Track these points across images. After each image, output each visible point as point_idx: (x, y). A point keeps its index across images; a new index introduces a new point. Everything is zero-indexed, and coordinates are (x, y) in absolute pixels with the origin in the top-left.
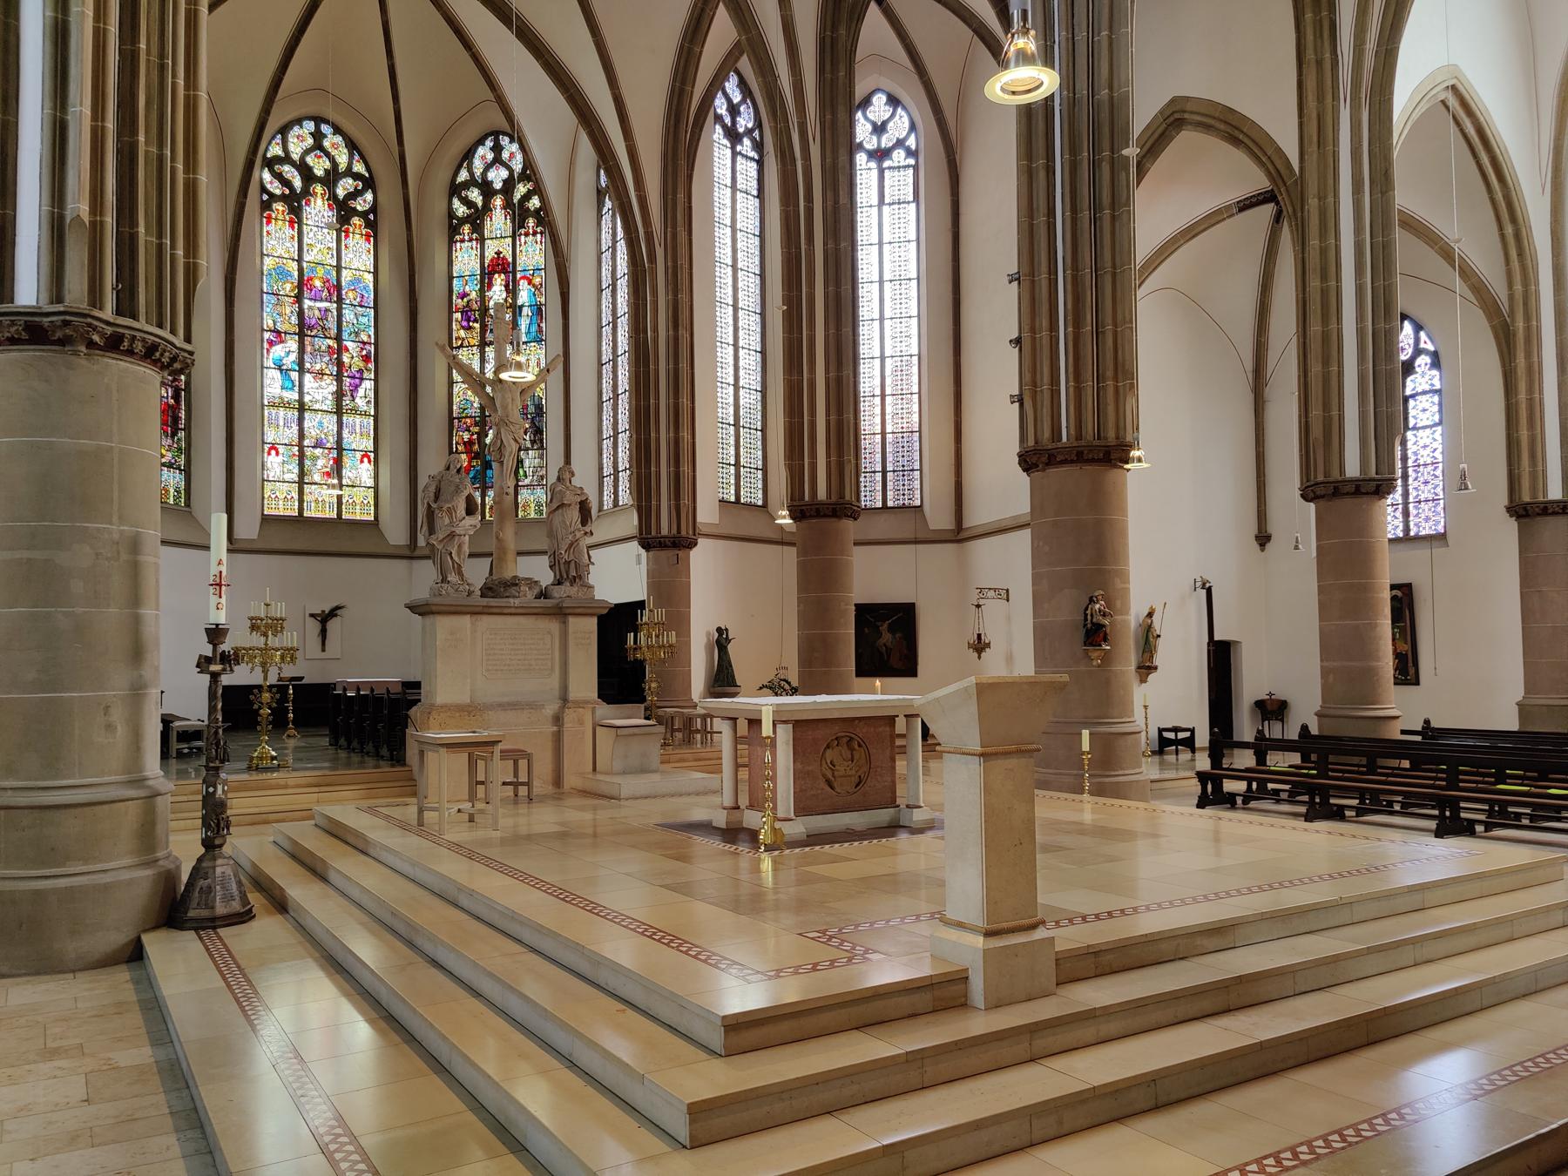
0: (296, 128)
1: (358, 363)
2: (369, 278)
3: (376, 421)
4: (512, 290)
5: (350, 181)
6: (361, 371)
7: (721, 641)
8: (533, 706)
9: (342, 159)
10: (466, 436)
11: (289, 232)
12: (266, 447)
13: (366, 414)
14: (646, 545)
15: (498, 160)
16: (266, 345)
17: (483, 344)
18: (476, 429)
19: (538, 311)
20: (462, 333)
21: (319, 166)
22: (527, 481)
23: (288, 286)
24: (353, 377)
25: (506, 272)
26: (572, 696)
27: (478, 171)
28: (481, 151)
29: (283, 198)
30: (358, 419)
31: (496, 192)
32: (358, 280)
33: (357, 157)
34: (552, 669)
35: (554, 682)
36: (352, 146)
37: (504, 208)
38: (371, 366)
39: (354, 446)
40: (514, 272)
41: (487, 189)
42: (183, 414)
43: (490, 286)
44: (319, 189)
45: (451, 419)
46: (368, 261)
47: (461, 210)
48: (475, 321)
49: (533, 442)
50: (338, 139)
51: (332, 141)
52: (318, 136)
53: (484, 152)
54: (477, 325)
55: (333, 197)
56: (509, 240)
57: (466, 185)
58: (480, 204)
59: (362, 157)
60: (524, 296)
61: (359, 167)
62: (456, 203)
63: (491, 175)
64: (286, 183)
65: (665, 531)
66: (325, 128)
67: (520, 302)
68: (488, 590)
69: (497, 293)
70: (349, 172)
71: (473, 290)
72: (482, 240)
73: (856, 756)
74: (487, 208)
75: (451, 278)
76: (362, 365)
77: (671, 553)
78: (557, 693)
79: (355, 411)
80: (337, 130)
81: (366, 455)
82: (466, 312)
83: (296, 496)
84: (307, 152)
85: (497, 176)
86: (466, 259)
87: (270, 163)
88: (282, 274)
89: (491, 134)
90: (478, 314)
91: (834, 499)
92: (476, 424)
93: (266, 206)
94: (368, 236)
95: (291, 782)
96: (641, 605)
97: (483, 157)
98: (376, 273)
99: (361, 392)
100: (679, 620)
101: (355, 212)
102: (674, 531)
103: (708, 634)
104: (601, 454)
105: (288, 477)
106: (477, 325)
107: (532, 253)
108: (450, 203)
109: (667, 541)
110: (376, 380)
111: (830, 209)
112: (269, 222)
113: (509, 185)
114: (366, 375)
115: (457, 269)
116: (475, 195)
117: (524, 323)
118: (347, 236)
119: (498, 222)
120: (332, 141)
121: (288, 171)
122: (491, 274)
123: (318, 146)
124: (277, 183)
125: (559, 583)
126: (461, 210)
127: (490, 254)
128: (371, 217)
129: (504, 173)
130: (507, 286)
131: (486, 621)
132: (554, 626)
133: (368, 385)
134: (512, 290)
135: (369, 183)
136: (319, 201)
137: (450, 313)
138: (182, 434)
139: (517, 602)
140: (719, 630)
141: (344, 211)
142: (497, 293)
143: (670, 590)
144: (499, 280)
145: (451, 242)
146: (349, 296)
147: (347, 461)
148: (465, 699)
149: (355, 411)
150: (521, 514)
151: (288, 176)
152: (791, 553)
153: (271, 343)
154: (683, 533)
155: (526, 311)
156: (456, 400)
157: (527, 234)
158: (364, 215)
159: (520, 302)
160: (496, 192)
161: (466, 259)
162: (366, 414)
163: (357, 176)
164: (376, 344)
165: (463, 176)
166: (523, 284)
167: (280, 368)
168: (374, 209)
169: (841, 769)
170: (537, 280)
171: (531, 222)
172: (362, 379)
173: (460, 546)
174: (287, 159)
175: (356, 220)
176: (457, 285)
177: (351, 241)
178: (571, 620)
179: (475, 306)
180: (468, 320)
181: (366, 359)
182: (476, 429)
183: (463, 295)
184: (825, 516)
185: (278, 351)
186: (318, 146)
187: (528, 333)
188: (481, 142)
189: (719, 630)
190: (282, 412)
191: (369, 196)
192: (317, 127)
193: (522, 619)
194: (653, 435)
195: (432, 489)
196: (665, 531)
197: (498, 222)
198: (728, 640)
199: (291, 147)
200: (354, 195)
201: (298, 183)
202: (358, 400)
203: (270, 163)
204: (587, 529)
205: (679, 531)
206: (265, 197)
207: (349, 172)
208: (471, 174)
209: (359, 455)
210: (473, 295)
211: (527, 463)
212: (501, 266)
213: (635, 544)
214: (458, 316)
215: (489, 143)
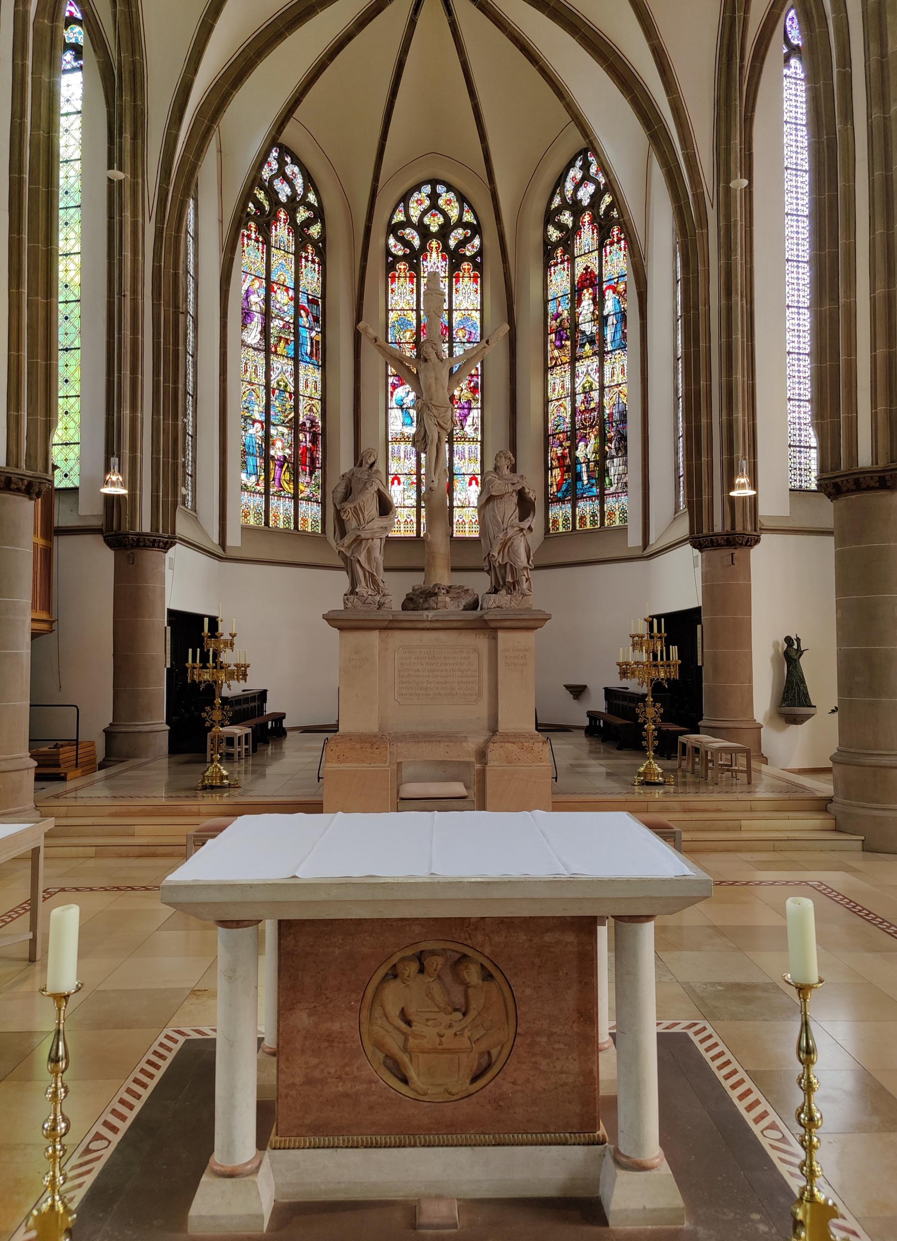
0: (415, 195)
1: (467, 394)
2: (476, 315)
3: (482, 445)
4: (599, 302)
5: (460, 231)
6: (469, 402)
7: (791, 654)
8: (452, 738)
9: (454, 213)
10: (559, 451)
11: (409, 286)
12: (390, 478)
13: (474, 440)
14: (698, 544)
15: (587, 178)
16: (390, 389)
17: (575, 359)
18: (568, 444)
19: (623, 316)
20: (556, 353)
21: (434, 223)
22: (612, 489)
23: (408, 334)
24: (463, 408)
25: (592, 285)
26: (502, 728)
27: (569, 194)
28: (572, 173)
29: (405, 257)
30: (467, 446)
31: (584, 210)
32: (466, 319)
33: (466, 208)
34: (479, 694)
35: (482, 709)
36: (462, 199)
37: (591, 223)
38: (478, 396)
39: (463, 471)
40: (601, 283)
41: (576, 208)
42: (319, 455)
43: (580, 301)
44: (434, 244)
45: (546, 437)
46: (474, 300)
47: (554, 234)
48: (567, 339)
49: (617, 450)
50: (451, 195)
51: (446, 197)
52: (434, 196)
53: (576, 173)
54: (568, 343)
55: (446, 247)
56: (596, 254)
57: (559, 210)
58: (570, 225)
59: (471, 207)
60: (610, 306)
61: (468, 217)
62: (551, 229)
63: (580, 194)
64: (407, 244)
65: (718, 528)
66: (440, 189)
67: (605, 313)
68: (411, 602)
69: (586, 306)
70: (460, 223)
71: (564, 309)
72: (572, 260)
73: (476, 1003)
74: (576, 229)
75: (546, 302)
76: (470, 396)
77: (726, 552)
78: (485, 723)
79: (464, 438)
80: (450, 188)
81: (474, 478)
82: (558, 332)
83: (414, 520)
84: (424, 213)
85: (585, 194)
86: (560, 281)
87: (393, 229)
88: (403, 324)
89: (579, 154)
90: (569, 332)
91: (882, 464)
92: (568, 439)
93: (390, 267)
94: (475, 277)
95: (204, 809)
96: (697, 611)
97: (574, 178)
98: (482, 311)
99: (469, 420)
100: (741, 632)
101: (464, 258)
102: (728, 527)
103: (776, 644)
104: (677, 453)
105: (409, 502)
106: (568, 343)
107: (617, 262)
108: (545, 230)
109: (724, 538)
110: (482, 408)
111: (873, 66)
112: (393, 281)
113: (596, 198)
114: (473, 406)
115: (552, 292)
116: (567, 218)
117: (609, 332)
118: (457, 281)
119: (587, 238)
120: (446, 197)
121: (411, 234)
122: (580, 291)
123: (434, 206)
124: (400, 246)
125: (496, 591)
126: (554, 234)
127: (579, 271)
128: (478, 260)
129: (591, 188)
130: (594, 299)
131: (398, 638)
132: (481, 642)
133: (476, 413)
134: (599, 302)
135: (476, 229)
136: (434, 255)
137: (546, 335)
138: (318, 473)
139: (430, 614)
140: (788, 640)
141: (455, 259)
142: (586, 306)
143: (727, 593)
144: (587, 295)
145: (547, 267)
146: (459, 335)
147: (458, 486)
148: (373, 727)
149: (464, 438)
150: (607, 522)
151: (409, 238)
152: (829, 543)
153: (395, 387)
154: (739, 528)
155: (611, 320)
156: (551, 418)
157: (612, 244)
158: (472, 259)
159: (605, 313)
160: (584, 210)
161: (560, 281)
162: (474, 440)
163: (466, 226)
164: (482, 375)
165: (557, 201)
166: (609, 294)
167: (401, 407)
168: (480, 252)
169: (427, 1032)
170: (621, 287)
171: (616, 231)
172: (470, 409)
173: (369, 552)
174: (408, 223)
175: (465, 265)
176: (552, 307)
177: (460, 286)
178: (501, 635)
179: (567, 325)
180: (561, 340)
181: (474, 390)
182: (568, 444)
183: (557, 316)
184: (869, 488)
185: (400, 392)
186: (434, 206)
187: (613, 341)
188: (571, 165)
189: (788, 640)
190: (403, 446)
191: (477, 242)
192: (434, 189)
193: (442, 636)
194: (704, 421)
195: (341, 490)
196: (718, 528)
197: (587, 238)
198: (800, 652)
199: (412, 212)
200: (462, 243)
201: (416, 243)
202: (467, 429)
203: (393, 229)
204: (525, 525)
205: (733, 528)
206: (390, 259)
207: (460, 223)
208: (563, 198)
209: (467, 478)
210: (565, 314)
211: (612, 472)
212: (591, 281)
213: (688, 547)
214: (553, 337)
215: (579, 163)
